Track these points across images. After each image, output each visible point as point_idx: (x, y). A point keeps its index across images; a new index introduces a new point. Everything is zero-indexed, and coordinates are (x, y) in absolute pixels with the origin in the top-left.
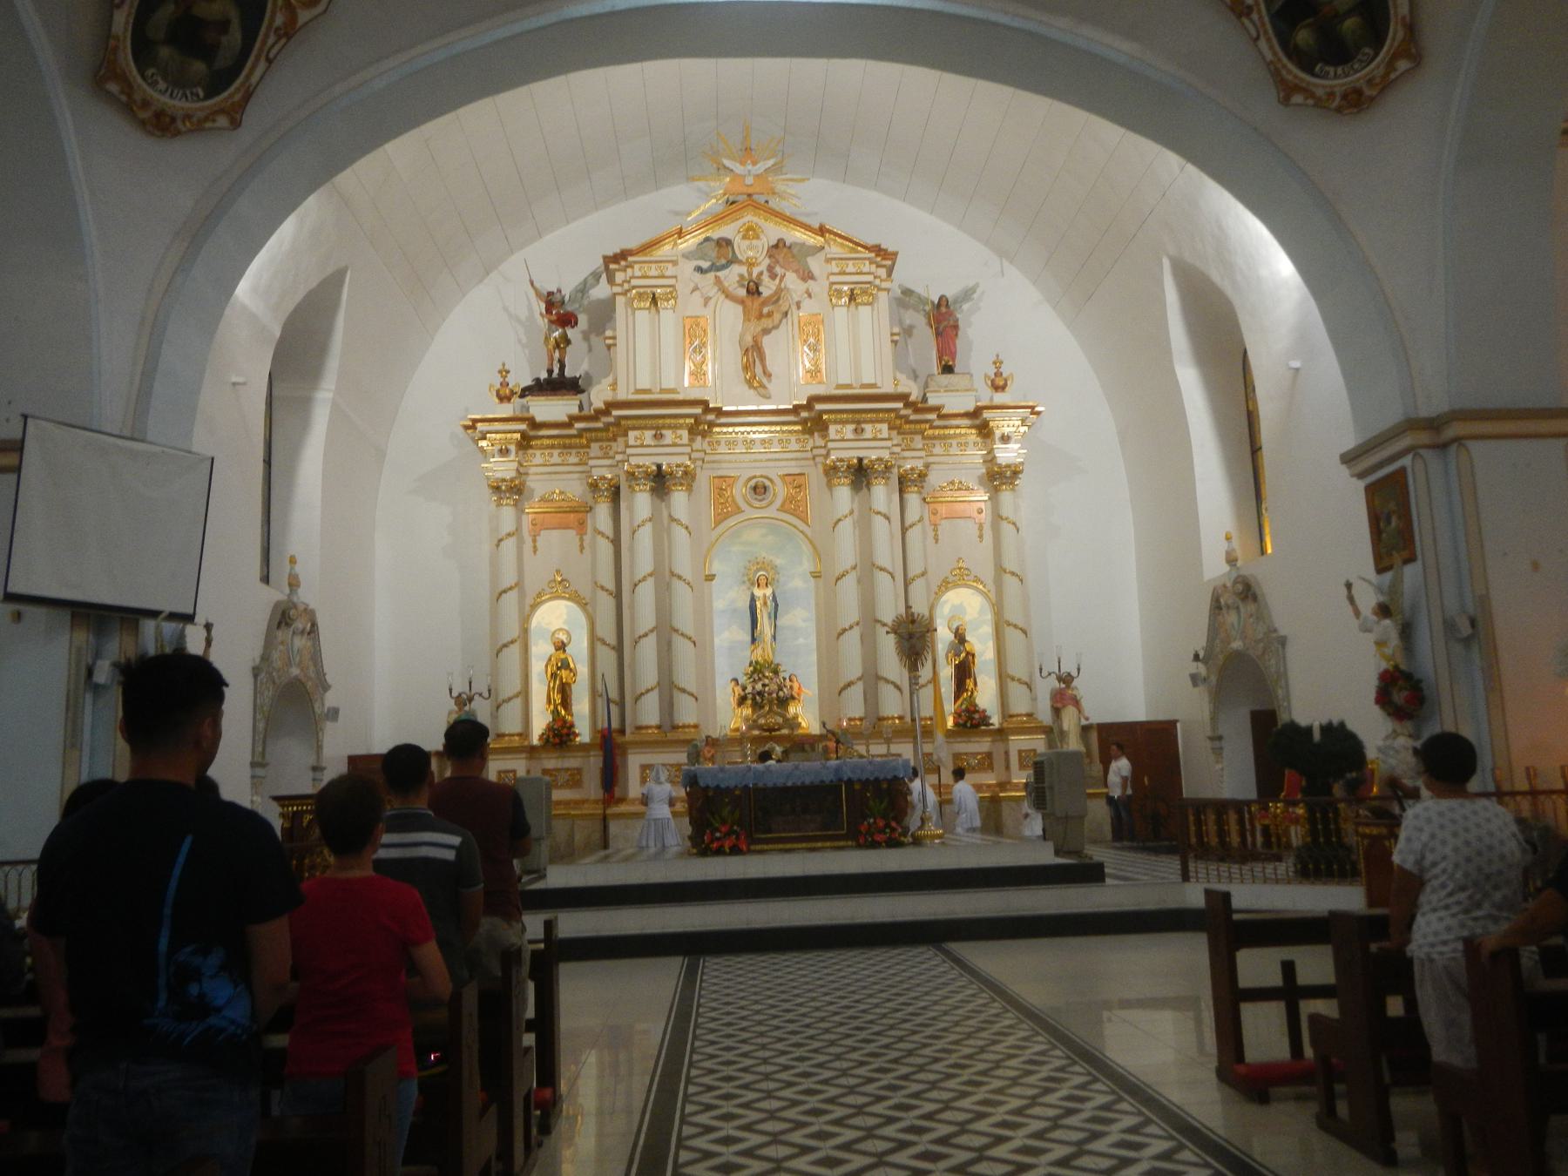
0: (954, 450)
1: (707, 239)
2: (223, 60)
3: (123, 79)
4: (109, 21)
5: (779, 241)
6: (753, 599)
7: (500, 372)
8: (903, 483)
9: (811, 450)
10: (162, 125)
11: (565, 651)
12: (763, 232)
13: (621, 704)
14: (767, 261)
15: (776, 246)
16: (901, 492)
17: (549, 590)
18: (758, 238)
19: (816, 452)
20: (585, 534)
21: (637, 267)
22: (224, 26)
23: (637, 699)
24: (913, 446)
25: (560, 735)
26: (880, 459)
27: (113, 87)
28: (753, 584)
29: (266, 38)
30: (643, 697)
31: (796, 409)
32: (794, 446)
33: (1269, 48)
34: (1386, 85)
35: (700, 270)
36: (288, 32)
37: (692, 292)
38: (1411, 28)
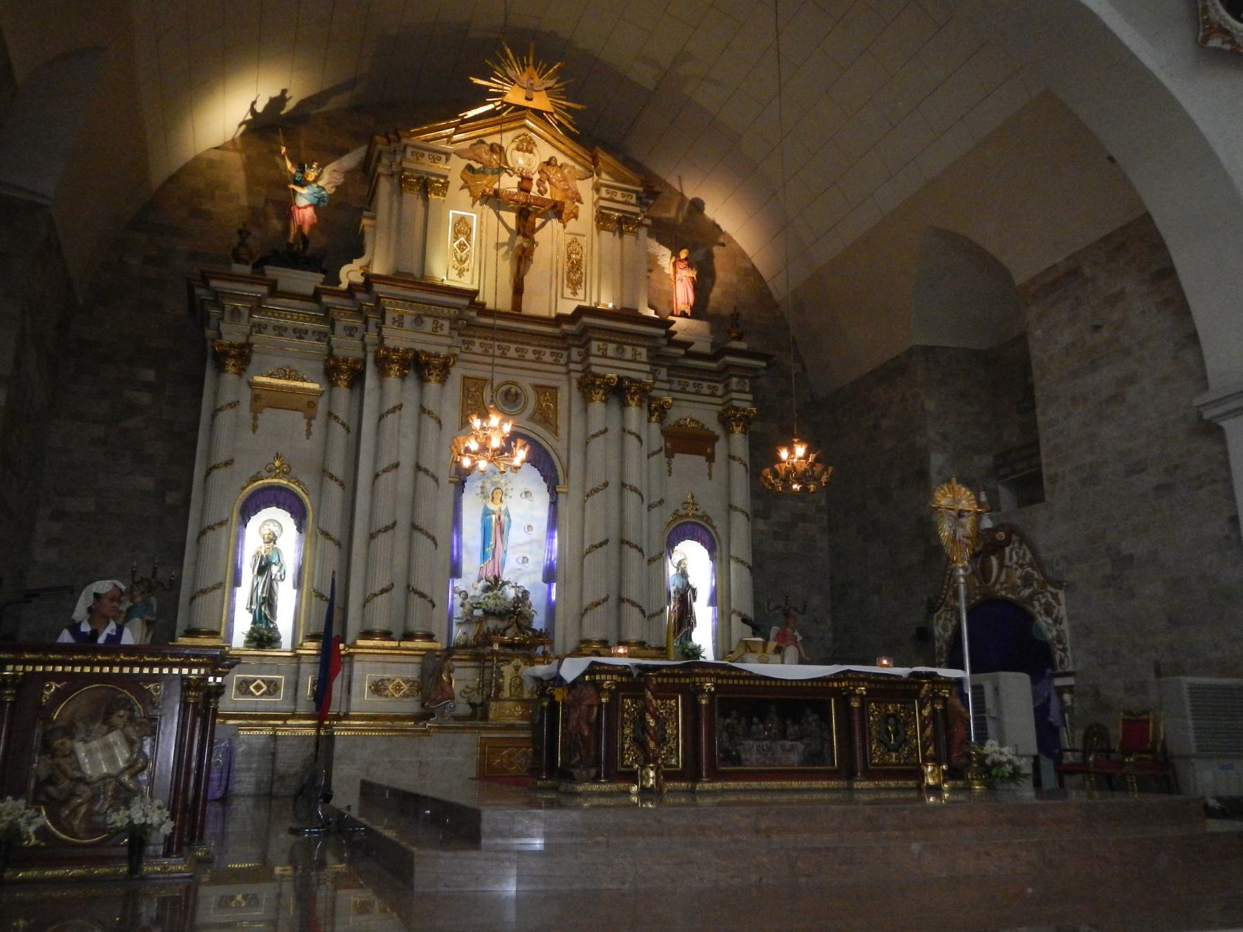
0: (691, 388)
1: (483, 142)
5: (551, 159)
6: (487, 513)
7: (240, 232)
9: (566, 365)
11: (275, 543)
12: (536, 146)
14: (536, 177)
15: (548, 163)
17: (264, 473)
18: (531, 152)
19: (572, 366)
20: (314, 418)
21: (409, 150)
24: (660, 377)
25: (263, 637)
26: (640, 382)
28: (485, 498)
30: (375, 599)
31: (560, 319)
32: (547, 357)
35: (469, 168)
37: (461, 189)
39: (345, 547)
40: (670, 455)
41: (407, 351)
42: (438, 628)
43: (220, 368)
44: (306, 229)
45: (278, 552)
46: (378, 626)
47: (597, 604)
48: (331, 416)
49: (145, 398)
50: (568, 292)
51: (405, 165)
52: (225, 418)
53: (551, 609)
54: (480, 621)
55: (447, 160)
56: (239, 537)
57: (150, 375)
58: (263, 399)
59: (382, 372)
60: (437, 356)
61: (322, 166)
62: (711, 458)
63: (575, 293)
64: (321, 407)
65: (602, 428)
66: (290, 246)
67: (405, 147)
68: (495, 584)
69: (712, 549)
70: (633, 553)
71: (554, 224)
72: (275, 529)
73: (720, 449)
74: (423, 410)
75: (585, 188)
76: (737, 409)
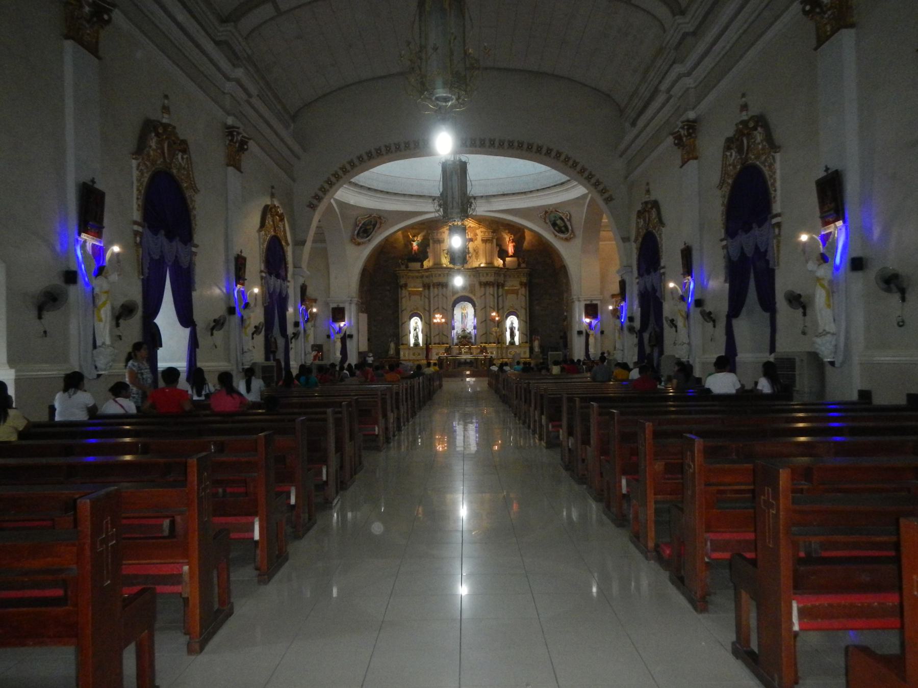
2: (369, 233)
3: (355, 239)
4: (354, 233)
6: (462, 313)
8: (498, 286)
10: (359, 244)
13: (430, 338)
16: (498, 288)
23: (434, 337)
25: (416, 344)
27: (353, 241)
29: (376, 228)
31: (473, 269)
32: (472, 276)
33: (552, 228)
34: (570, 238)
36: (379, 228)
38: (573, 231)
39: (430, 325)
40: (506, 296)
41: (437, 283)
42: (450, 341)
43: (402, 289)
45: (418, 326)
46: (437, 342)
47: (484, 334)
50: (475, 260)
52: (404, 300)
53: (475, 336)
54: (461, 339)
55: (444, 232)
56: (410, 324)
57: (388, 288)
58: (411, 294)
59: (434, 288)
61: (417, 237)
62: (517, 294)
67: (434, 233)
68: (464, 330)
69: (518, 317)
71: (471, 243)
72: (416, 320)
73: (520, 291)
74: (443, 295)
75: (478, 232)
76: (521, 282)
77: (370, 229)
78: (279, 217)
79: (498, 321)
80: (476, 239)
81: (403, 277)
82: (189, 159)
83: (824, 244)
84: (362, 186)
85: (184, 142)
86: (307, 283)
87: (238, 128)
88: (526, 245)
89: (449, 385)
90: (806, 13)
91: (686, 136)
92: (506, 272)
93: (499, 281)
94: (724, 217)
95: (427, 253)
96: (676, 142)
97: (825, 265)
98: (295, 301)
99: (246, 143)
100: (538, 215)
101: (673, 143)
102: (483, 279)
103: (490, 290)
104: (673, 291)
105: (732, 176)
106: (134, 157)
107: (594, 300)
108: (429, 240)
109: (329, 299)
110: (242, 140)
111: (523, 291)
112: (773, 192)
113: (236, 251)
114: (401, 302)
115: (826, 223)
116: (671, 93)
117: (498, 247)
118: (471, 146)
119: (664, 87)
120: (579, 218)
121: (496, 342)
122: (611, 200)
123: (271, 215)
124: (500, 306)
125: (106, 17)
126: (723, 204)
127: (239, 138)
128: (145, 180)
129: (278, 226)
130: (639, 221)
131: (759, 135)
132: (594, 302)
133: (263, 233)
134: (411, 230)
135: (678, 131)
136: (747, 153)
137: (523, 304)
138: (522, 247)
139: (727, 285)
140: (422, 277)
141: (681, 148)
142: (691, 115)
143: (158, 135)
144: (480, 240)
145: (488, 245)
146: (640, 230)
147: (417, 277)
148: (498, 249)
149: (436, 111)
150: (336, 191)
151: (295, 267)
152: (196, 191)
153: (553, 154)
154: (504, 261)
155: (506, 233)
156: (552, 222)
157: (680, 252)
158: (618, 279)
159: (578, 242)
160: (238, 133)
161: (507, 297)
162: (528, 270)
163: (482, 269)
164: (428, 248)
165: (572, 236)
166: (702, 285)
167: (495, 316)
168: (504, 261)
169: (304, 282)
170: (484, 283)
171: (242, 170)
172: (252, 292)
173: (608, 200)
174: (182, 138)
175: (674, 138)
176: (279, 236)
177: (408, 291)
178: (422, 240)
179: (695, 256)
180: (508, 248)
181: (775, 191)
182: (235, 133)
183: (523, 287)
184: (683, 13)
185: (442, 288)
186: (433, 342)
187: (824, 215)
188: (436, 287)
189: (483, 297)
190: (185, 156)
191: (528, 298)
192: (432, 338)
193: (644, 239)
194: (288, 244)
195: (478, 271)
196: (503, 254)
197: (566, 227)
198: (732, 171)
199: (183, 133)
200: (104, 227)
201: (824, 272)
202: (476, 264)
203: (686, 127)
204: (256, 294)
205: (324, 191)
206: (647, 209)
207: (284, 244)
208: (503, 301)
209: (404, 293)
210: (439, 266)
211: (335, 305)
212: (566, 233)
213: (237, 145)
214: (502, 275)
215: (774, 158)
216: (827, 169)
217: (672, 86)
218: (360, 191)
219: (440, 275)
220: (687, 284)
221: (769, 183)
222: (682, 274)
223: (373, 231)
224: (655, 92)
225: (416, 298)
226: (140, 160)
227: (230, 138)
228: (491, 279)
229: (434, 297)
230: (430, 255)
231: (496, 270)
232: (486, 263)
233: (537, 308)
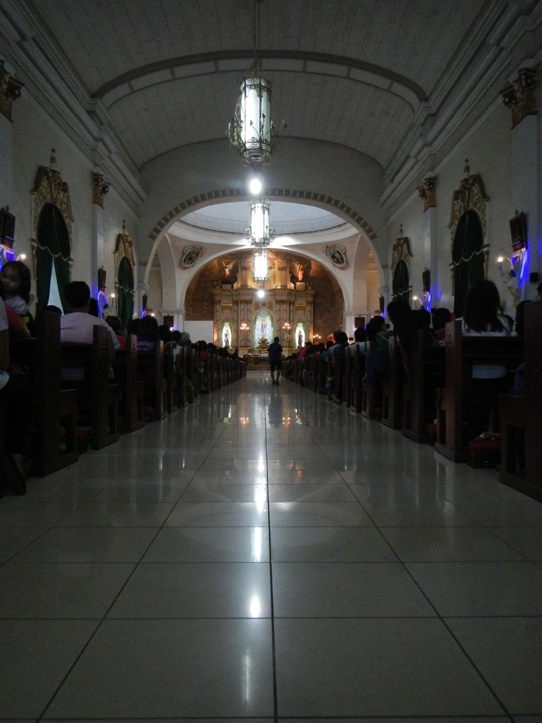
2: (193, 260)
3: (182, 264)
6: (262, 324)
10: (185, 268)
16: (290, 305)
22: (194, 257)
23: (241, 341)
27: (181, 266)
31: (271, 290)
33: (331, 260)
34: (345, 267)
36: (201, 256)
38: (347, 262)
39: (237, 332)
40: (296, 311)
41: (243, 300)
43: (216, 305)
44: (228, 275)
45: (228, 333)
46: (243, 345)
48: (234, 311)
49: (206, 308)
51: (242, 265)
52: (218, 313)
54: (261, 343)
55: (250, 262)
57: (206, 303)
58: (224, 308)
60: (249, 300)
61: (229, 265)
62: (304, 310)
63: (274, 283)
64: (233, 309)
65: (279, 309)
66: (226, 279)
67: (242, 262)
70: (285, 332)
72: (227, 329)
74: (248, 310)
75: (276, 262)
77: (194, 257)
78: (129, 243)
79: (289, 330)
80: (274, 268)
81: (218, 295)
82: (68, 197)
83: (514, 264)
84: (188, 224)
85: (65, 184)
86: (147, 295)
87: (102, 176)
88: (311, 272)
89: (251, 375)
90: (505, 103)
91: (428, 190)
92: (296, 293)
93: (291, 300)
94: (452, 248)
95: (237, 276)
96: (421, 194)
97: (514, 278)
98: (139, 307)
99: (107, 187)
100: (321, 249)
101: (419, 195)
102: (279, 298)
103: (285, 307)
104: (416, 302)
105: (458, 218)
106: (32, 193)
107: (362, 315)
108: (238, 268)
109: (161, 310)
110: (104, 185)
111: (309, 308)
112: (485, 230)
113: (99, 266)
114: (216, 313)
115: (515, 250)
116: (419, 157)
117: (290, 274)
118: (271, 195)
119: (412, 154)
120: (352, 252)
121: (288, 347)
122: (374, 238)
123: (123, 241)
124: (291, 319)
125: (17, 92)
126: (451, 239)
127: (102, 183)
128: (39, 210)
129: (127, 251)
130: (394, 252)
131: (476, 189)
132: (362, 316)
133: (117, 254)
134: (224, 260)
135: (423, 186)
136: (468, 202)
137: (309, 319)
138: (309, 273)
139: (453, 298)
140: (232, 295)
141: (424, 198)
142: (431, 174)
143: (48, 178)
144: (277, 269)
145: (283, 272)
146: (395, 260)
147: (228, 296)
148: (291, 276)
149: (250, 165)
150: (170, 226)
151: (139, 282)
152: (72, 220)
153: (333, 202)
154: (295, 285)
155: (297, 263)
156: (332, 255)
157: (421, 275)
158: (380, 296)
159: (350, 271)
160: (102, 180)
161: (297, 312)
162: (313, 292)
163: (277, 290)
164: (237, 273)
165: (346, 266)
166: (436, 298)
167: (287, 326)
168: (295, 285)
169: (146, 293)
170: (279, 301)
171: (103, 207)
172: (110, 297)
173: (373, 237)
174: (64, 181)
175: (420, 191)
176: (128, 258)
177: (222, 306)
178: (233, 267)
179: (432, 276)
180: (298, 276)
181: (486, 228)
182: (100, 180)
183: (309, 305)
184: (427, 99)
185: (248, 304)
186: (239, 345)
187: (515, 244)
188: (243, 304)
189: (279, 311)
190: (66, 195)
191: (312, 313)
192: (239, 342)
193: (398, 266)
194: (134, 264)
195: (275, 292)
196: (294, 279)
197: (342, 259)
198: (458, 215)
199: (64, 178)
200: (14, 241)
201: (513, 282)
202: (273, 287)
203: (427, 183)
204: (113, 298)
205: (162, 225)
206: (400, 244)
207: (131, 264)
208: (294, 317)
209: (218, 307)
210: (244, 288)
211: (166, 315)
212: (342, 263)
213: (101, 188)
214: (293, 296)
215: (485, 204)
216: (517, 212)
217: (419, 153)
218: (187, 228)
219: (246, 294)
220: (427, 297)
221: (482, 224)
222: (423, 290)
223: (195, 259)
224: (408, 157)
225: (227, 312)
226: (36, 196)
227: (96, 183)
228: (285, 298)
229: (241, 311)
230: (239, 280)
231: (289, 292)
232: (281, 286)
233: (320, 321)
